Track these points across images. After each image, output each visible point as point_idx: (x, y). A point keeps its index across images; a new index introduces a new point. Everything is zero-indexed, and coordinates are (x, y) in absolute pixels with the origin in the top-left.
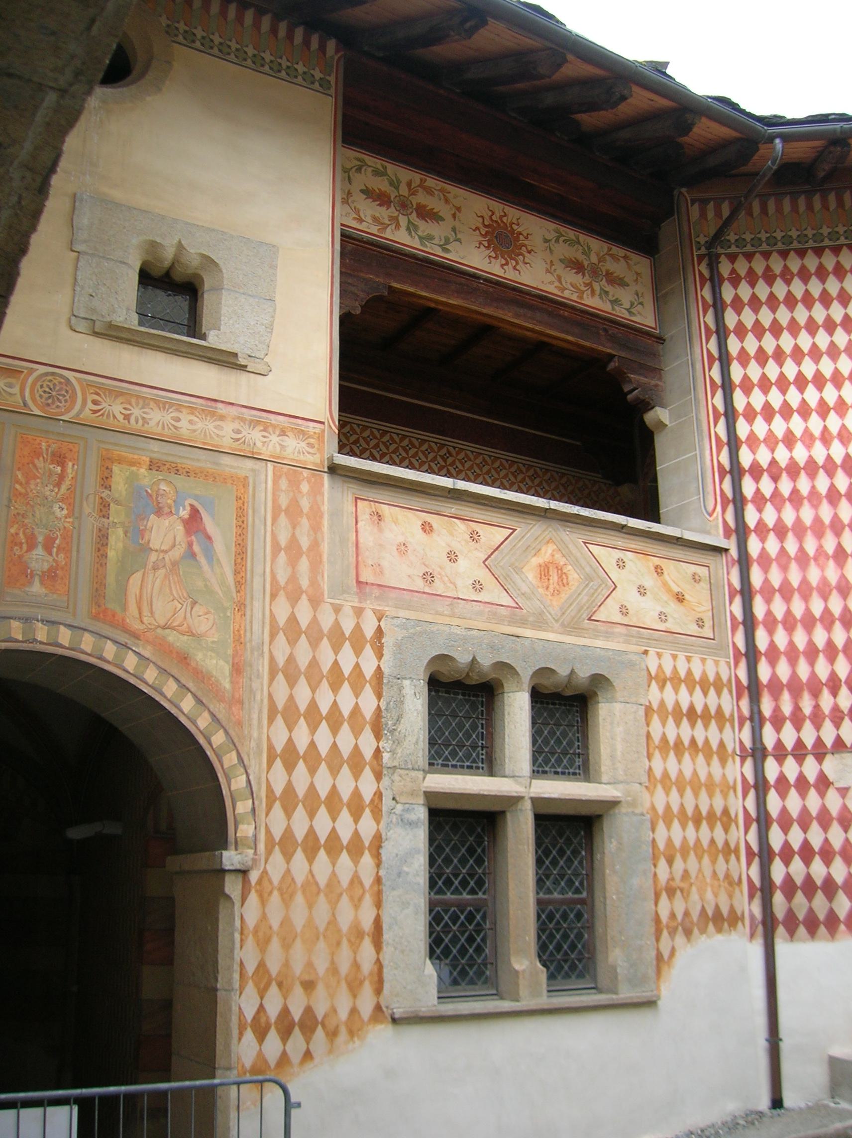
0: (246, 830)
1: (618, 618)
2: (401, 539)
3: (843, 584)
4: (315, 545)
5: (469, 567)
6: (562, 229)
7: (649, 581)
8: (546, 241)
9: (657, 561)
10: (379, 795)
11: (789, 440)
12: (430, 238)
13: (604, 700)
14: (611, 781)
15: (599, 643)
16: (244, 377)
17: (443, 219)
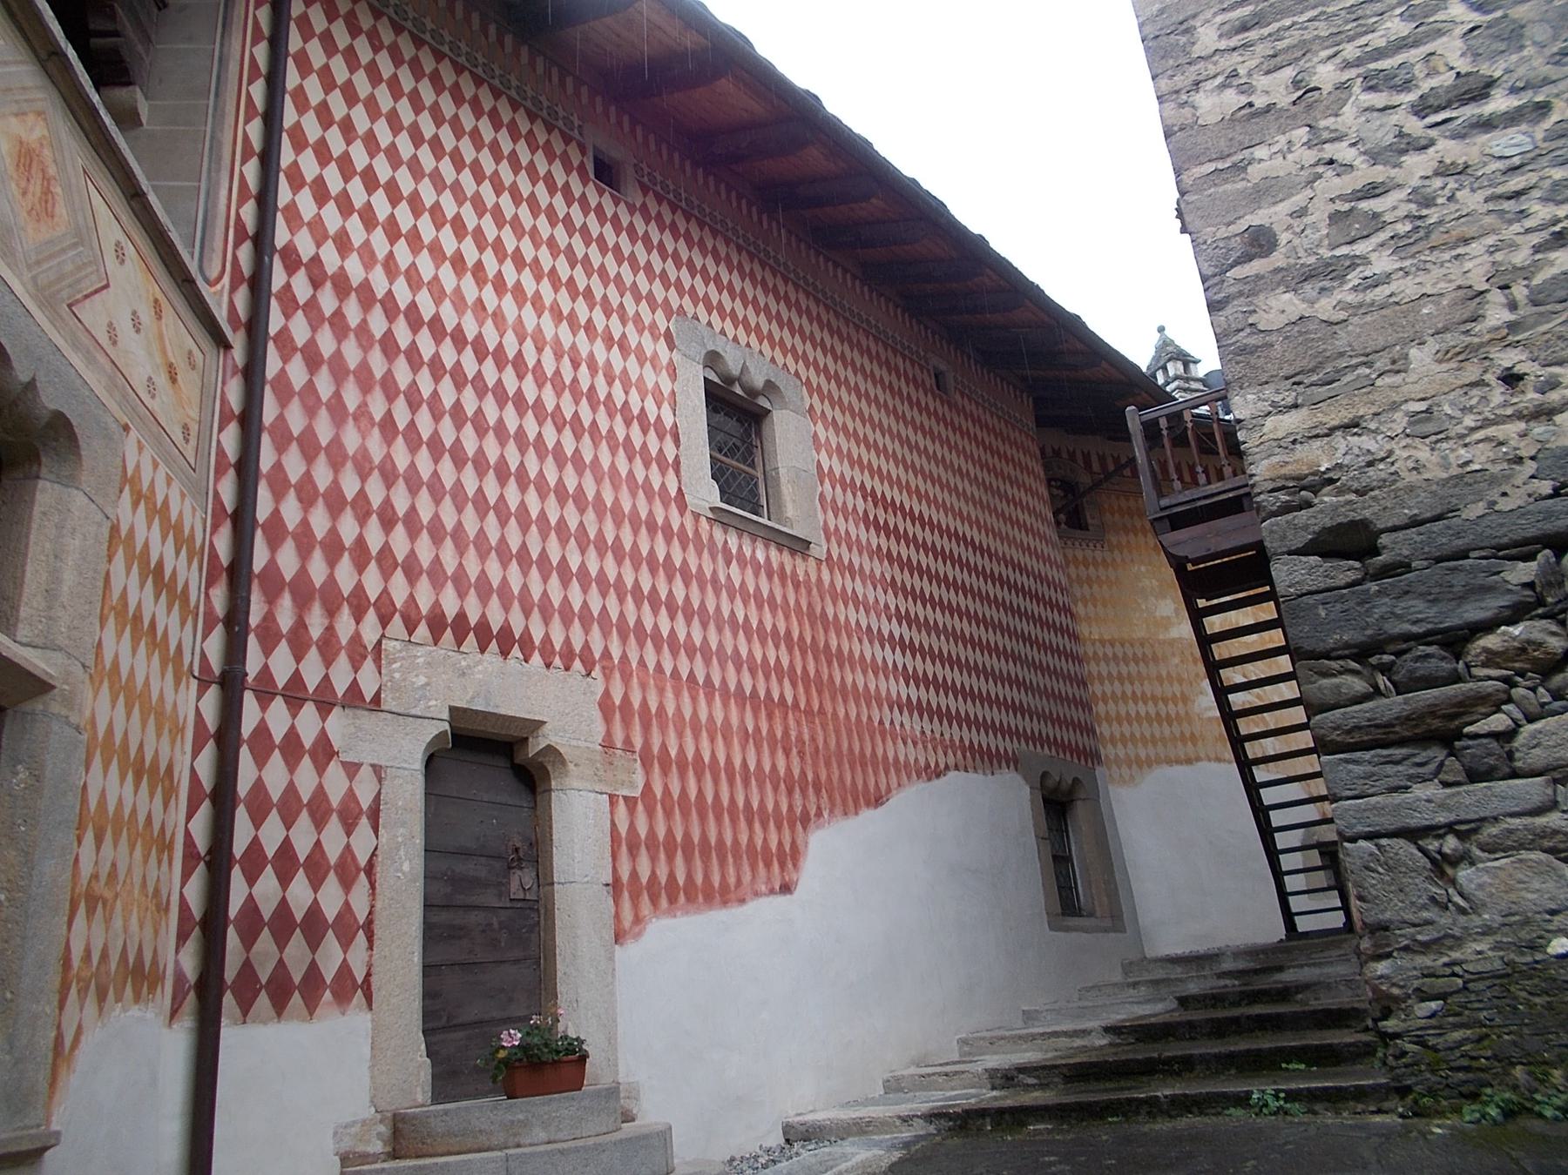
3: (389, 466)
11: (343, 243)
13: (52, 477)
14: (38, 641)
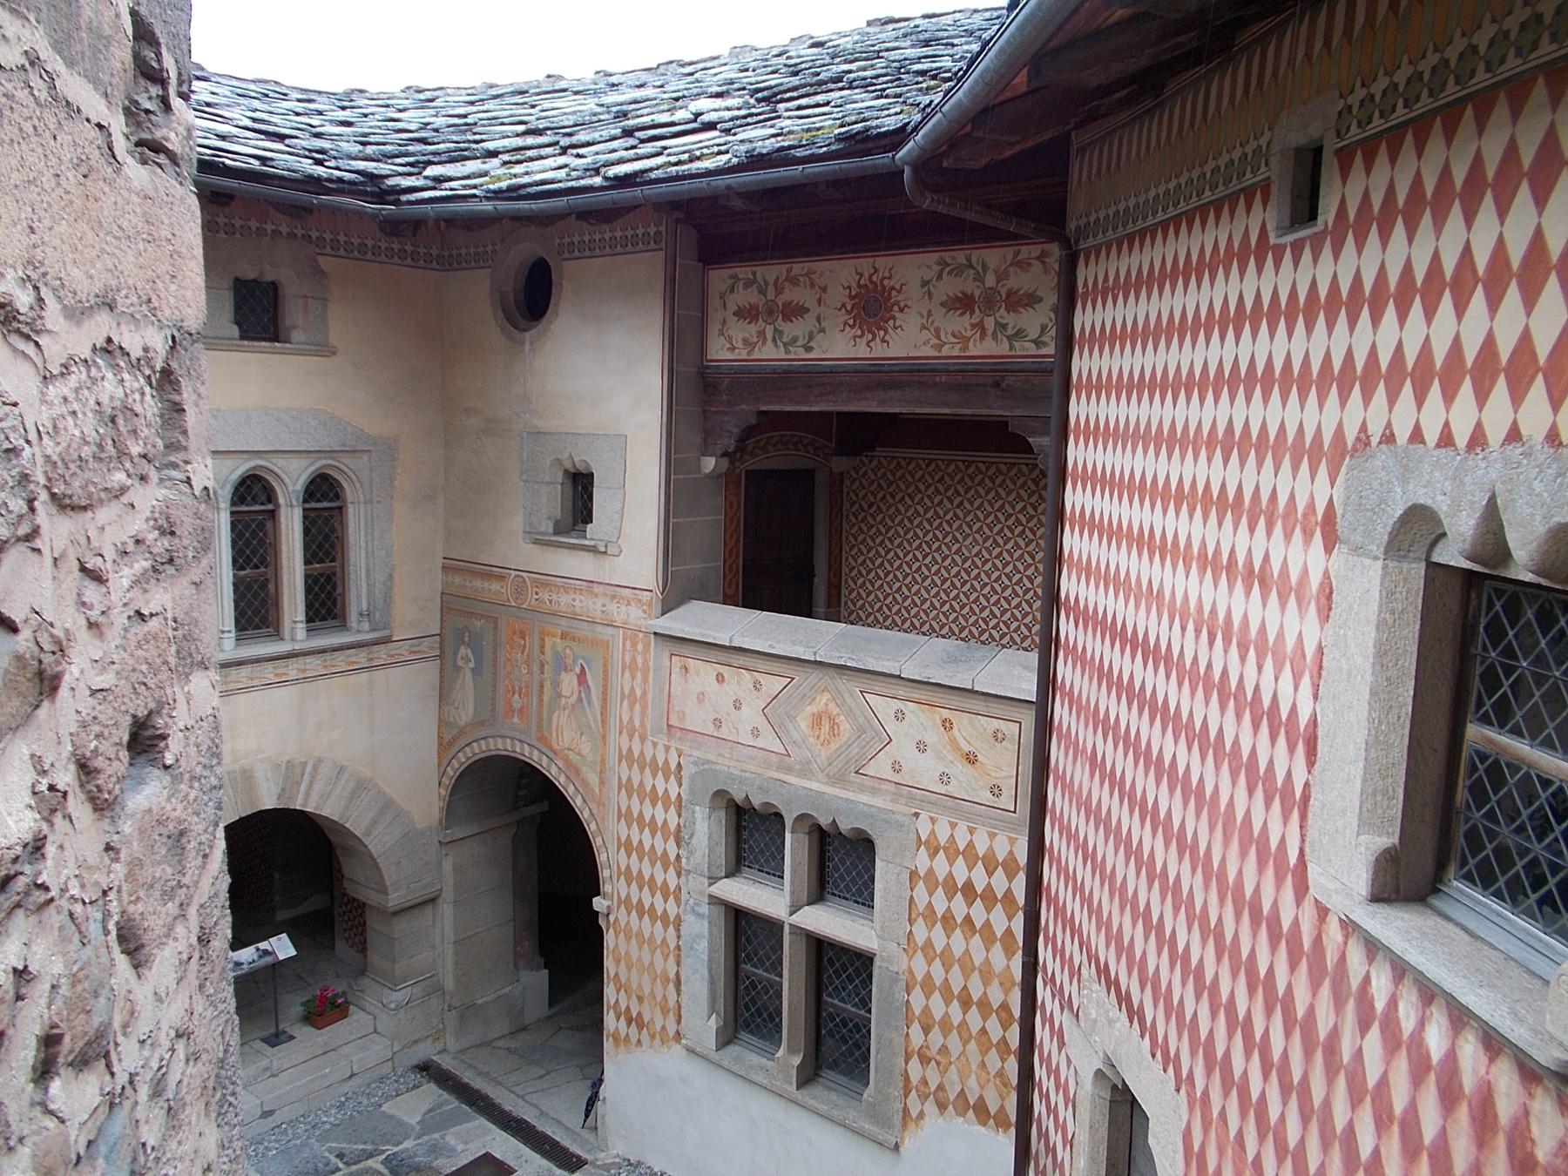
0: (607, 888)
1: (888, 774)
2: (700, 689)
4: (645, 693)
5: (750, 715)
6: (946, 256)
7: (934, 737)
8: (925, 284)
9: (946, 713)
10: (679, 888)
12: (794, 340)
15: (864, 798)
16: (607, 562)
17: (808, 310)
